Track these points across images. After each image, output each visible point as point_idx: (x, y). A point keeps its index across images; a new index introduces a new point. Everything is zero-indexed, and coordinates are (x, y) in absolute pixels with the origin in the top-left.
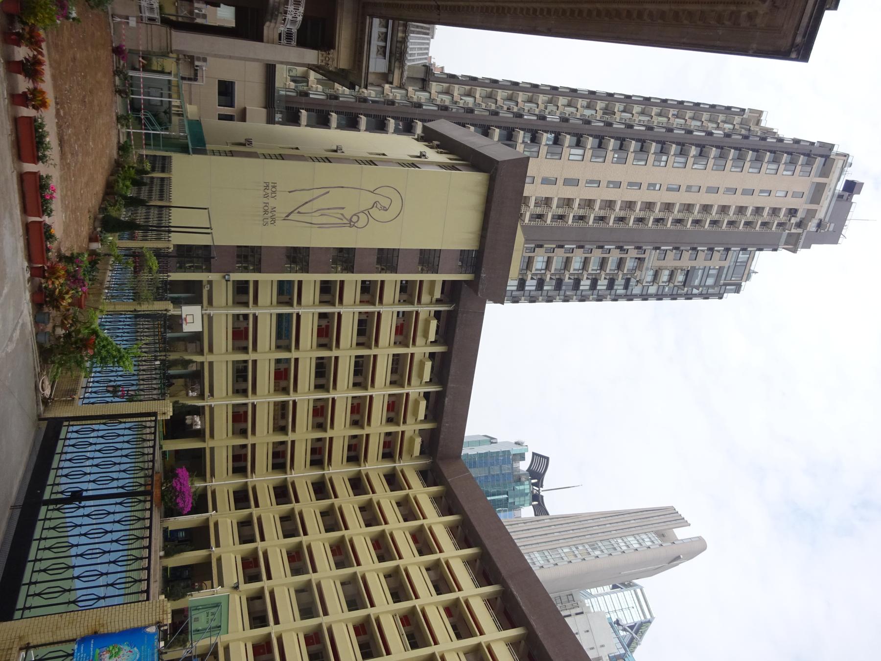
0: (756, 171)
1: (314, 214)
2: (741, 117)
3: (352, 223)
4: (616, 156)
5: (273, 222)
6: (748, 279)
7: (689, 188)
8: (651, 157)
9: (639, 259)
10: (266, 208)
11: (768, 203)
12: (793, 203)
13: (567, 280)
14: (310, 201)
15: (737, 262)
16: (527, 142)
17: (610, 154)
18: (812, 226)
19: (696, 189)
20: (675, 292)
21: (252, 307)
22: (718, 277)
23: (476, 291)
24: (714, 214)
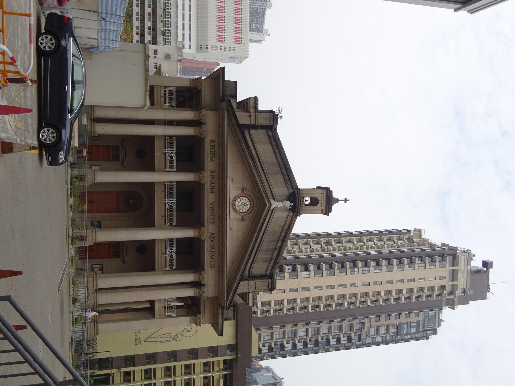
0: (413, 268)
1: (157, 338)
2: (408, 235)
3: (175, 339)
4: (329, 272)
5: (139, 343)
6: (439, 325)
7: (375, 283)
8: (349, 271)
9: (362, 323)
10: (136, 338)
11: (426, 285)
12: (443, 283)
13: (320, 340)
14: (156, 332)
15: (428, 316)
16: (277, 273)
17: (325, 272)
18: (459, 293)
19: (380, 283)
20: (394, 339)
21: (133, 382)
22: (418, 327)
23: (237, 363)
24: (394, 295)
